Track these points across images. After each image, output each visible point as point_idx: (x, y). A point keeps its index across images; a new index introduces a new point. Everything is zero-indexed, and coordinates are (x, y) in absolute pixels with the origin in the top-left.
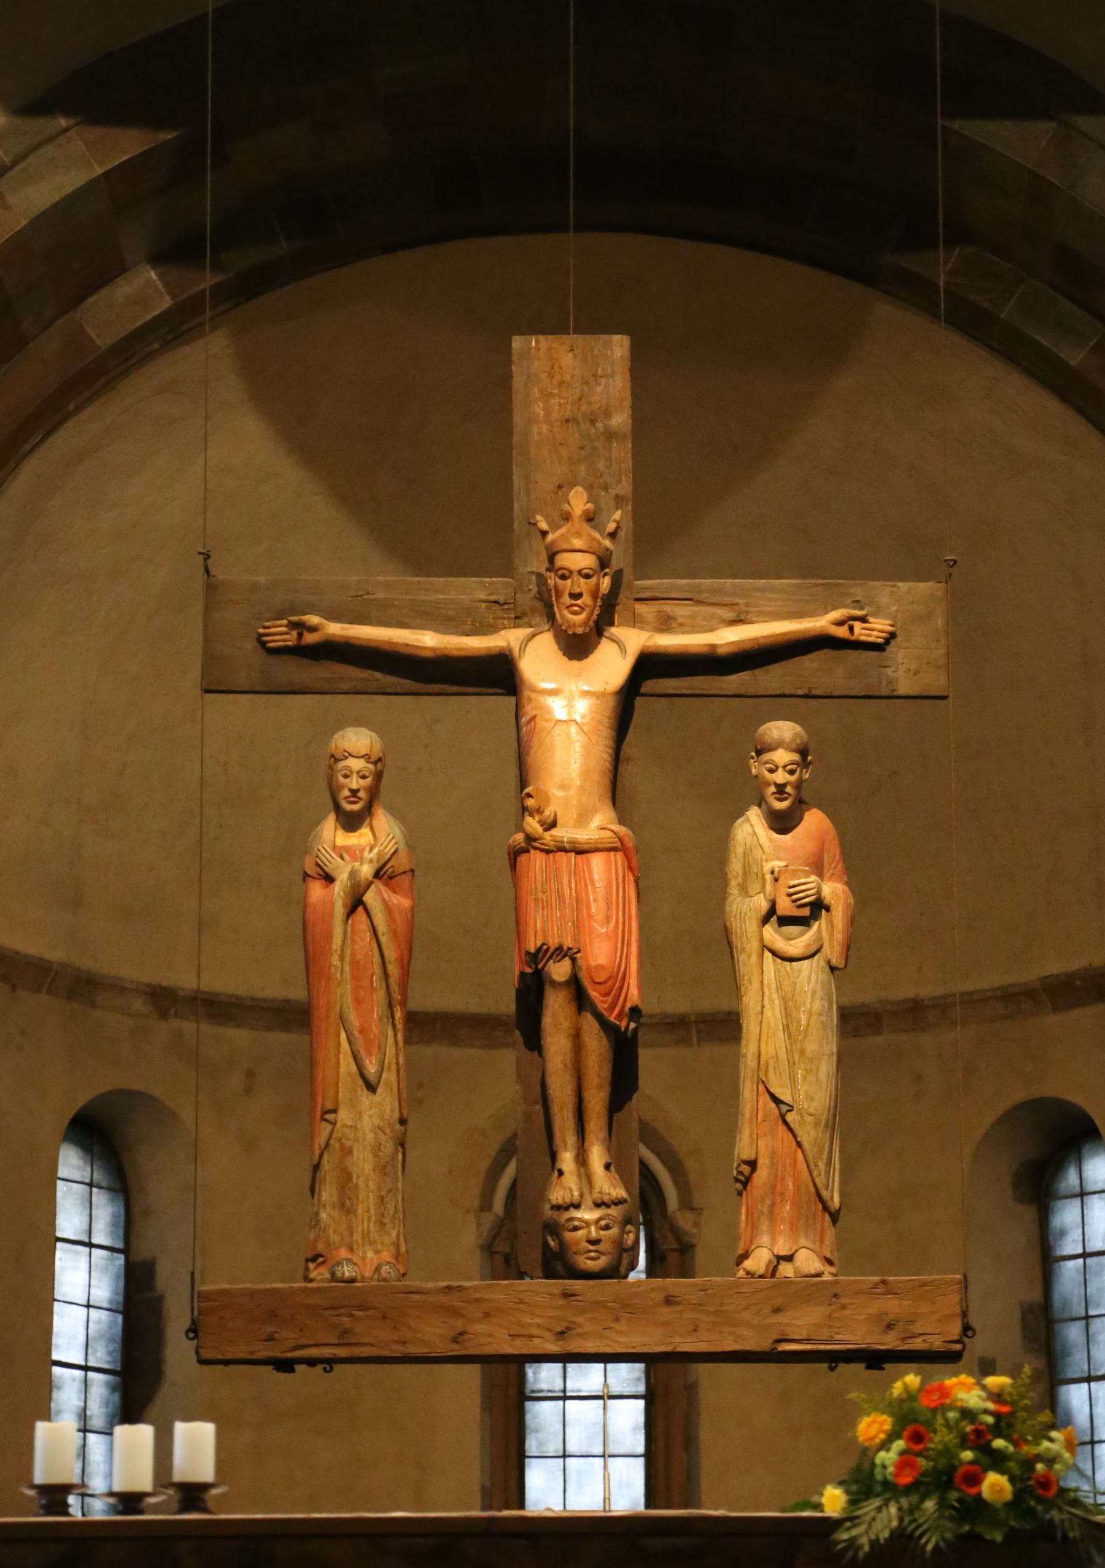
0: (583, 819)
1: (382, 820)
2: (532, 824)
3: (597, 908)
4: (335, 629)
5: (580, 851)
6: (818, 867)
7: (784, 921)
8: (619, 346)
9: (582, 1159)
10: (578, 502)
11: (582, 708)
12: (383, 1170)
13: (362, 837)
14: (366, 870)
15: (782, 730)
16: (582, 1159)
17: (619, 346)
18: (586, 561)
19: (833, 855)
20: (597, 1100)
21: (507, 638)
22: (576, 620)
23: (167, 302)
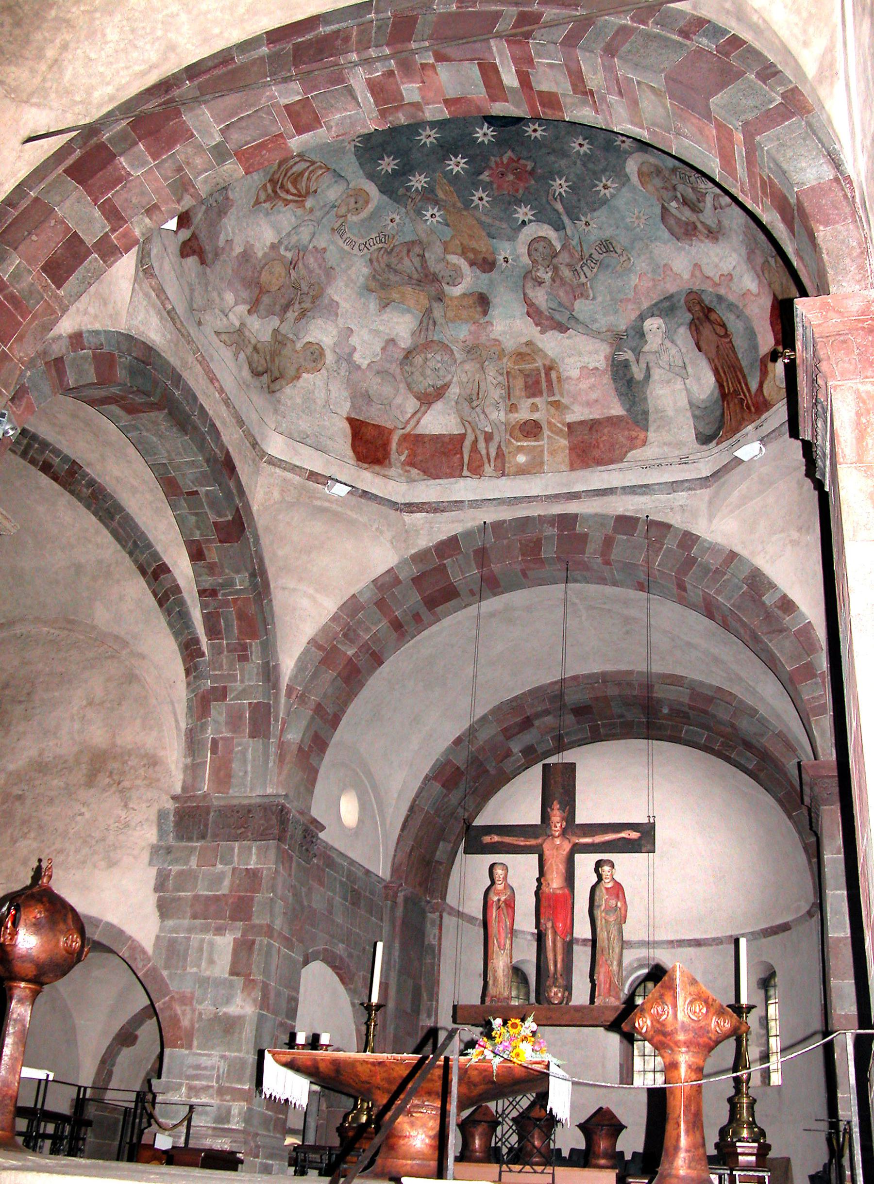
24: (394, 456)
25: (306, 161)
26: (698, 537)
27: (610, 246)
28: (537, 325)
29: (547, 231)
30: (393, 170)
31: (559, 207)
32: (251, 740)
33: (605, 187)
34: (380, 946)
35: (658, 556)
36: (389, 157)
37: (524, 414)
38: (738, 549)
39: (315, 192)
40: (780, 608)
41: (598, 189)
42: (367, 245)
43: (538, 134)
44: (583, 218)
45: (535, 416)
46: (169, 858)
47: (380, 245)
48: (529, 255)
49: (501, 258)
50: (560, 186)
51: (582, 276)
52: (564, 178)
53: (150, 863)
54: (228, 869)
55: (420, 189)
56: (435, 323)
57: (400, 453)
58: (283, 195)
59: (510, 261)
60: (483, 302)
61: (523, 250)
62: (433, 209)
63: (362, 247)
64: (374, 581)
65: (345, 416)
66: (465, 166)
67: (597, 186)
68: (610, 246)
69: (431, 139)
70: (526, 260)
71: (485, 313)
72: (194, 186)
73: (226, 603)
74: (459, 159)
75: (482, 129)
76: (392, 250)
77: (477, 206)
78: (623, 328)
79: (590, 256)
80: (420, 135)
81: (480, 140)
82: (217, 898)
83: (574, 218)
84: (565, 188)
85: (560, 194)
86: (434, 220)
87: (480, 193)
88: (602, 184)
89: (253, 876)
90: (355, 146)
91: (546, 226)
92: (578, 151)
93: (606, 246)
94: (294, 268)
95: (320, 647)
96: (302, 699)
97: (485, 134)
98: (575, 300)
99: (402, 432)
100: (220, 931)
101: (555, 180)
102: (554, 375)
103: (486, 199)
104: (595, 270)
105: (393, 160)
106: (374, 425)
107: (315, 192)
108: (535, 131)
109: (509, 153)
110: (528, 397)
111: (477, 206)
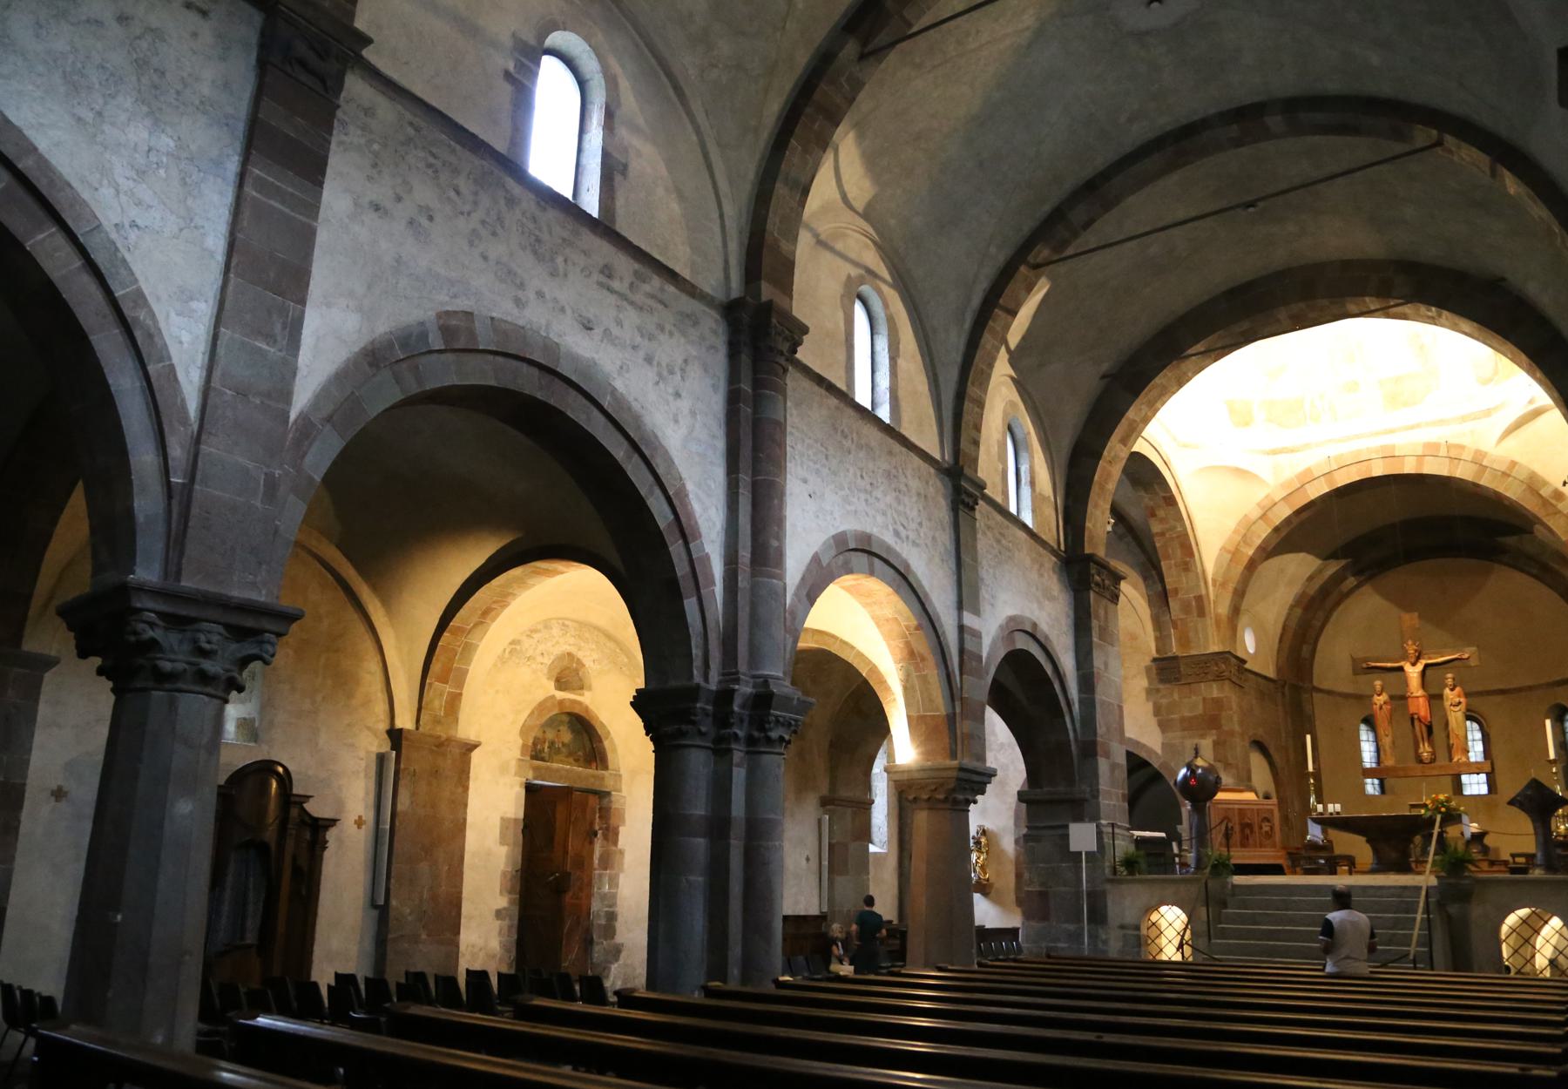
0: (1417, 692)
1: (1384, 694)
2: (1409, 694)
3: (1421, 707)
4: (1373, 664)
5: (1417, 697)
6: (1459, 696)
7: (1454, 706)
8: (1416, 614)
9: (1424, 745)
10: (1410, 642)
11: (1415, 675)
12: (1390, 748)
13: (1381, 697)
14: (1382, 703)
15: (1449, 675)
16: (1424, 745)
17: (1416, 614)
18: (1412, 652)
19: (1462, 693)
20: (1425, 735)
21: (1402, 664)
22: (1413, 660)
23: (1355, 583)
26: (1486, 453)
32: (1199, 619)
34: (1308, 738)
35: (1457, 468)
38: (1517, 459)
40: (1552, 498)
46: (1160, 695)
53: (1148, 700)
54: (1201, 697)
64: (1258, 504)
73: (1172, 539)
82: (1195, 717)
89: (1218, 703)
95: (1229, 552)
96: (1223, 585)
100: (1202, 736)
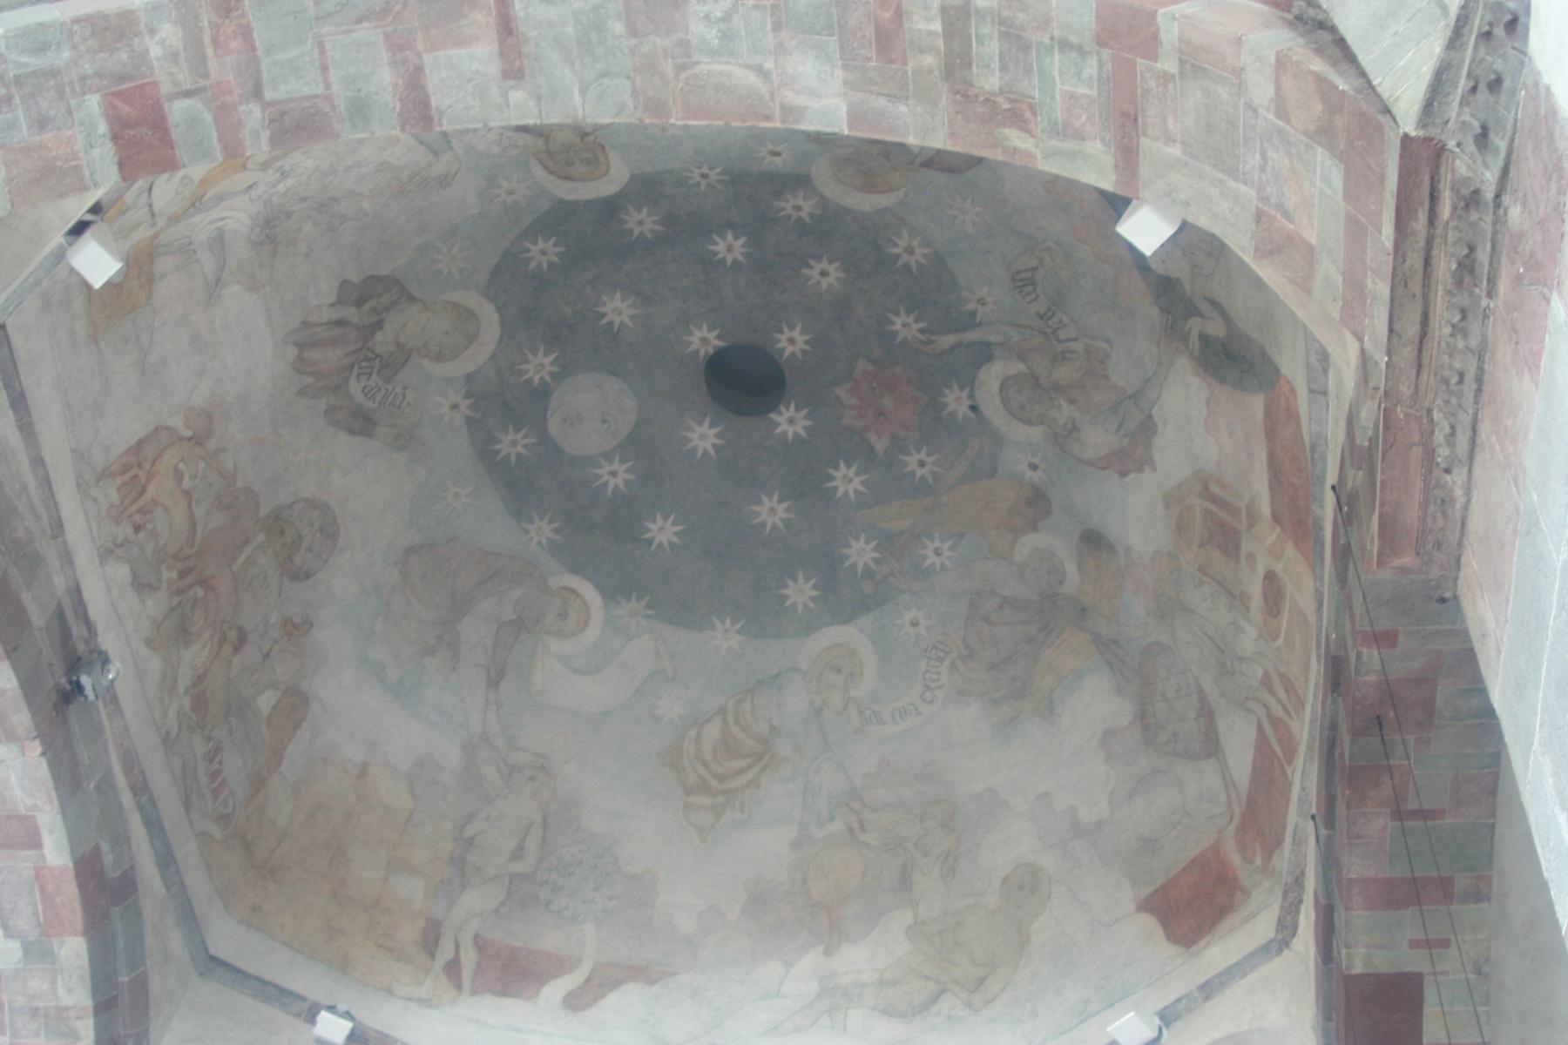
24: (1243, 874)
25: (708, 721)
27: (1023, 275)
28: (1140, 470)
29: (993, 375)
30: (815, 587)
31: (948, 340)
33: (910, 251)
36: (786, 587)
37: (1255, 588)
39: (773, 729)
41: (913, 264)
42: (933, 685)
43: (800, 339)
44: (972, 306)
45: (1261, 571)
47: (946, 664)
48: (1029, 423)
49: (1029, 473)
50: (905, 326)
51: (1073, 346)
52: (891, 316)
55: (876, 555)
56: (1115, 642)
57: (1248, 861)
58: (736, 783)
59: (1035, 460)
60: (1094, 541)
61: (1019, 432)
62: (925, 547)
63: (928, 696)
65: (1131, 907)
66: (854, 468)
67: (907, 266)
68: (1023, 275)
69: (781, 510)
70: (1036, 433)
71: (1111, 548)
72: (67, 1008)
74: (838, 474)
75: (778, 425)
76: (967, 646)
77: (933, 473)
78: (1155, 311)
79: (1042, 317)
80: (763, 524)
81: (803, 433)
83: (971, 321)
84: (910, 320)
85: (922, 331)
86: (947, 553)
87: (912, 461)
88: (906, 257)
90: (739, 632)
91: (983, 374)
92: (838, 279)
93: (1024, 281)
94: (863, 829)
97: (791, 421)
98: (1106, 377)
99: (1232, 828)
101: (895, 334)
102: (1215, 489)
103: (923, 456)
104: (1065, 320)
105: (795, 580)
106: (1184, 870)
107: (773, 729)
108: (792, 341)
109: (841, 391)
110: (1237, 561)
111: (933, 473)
